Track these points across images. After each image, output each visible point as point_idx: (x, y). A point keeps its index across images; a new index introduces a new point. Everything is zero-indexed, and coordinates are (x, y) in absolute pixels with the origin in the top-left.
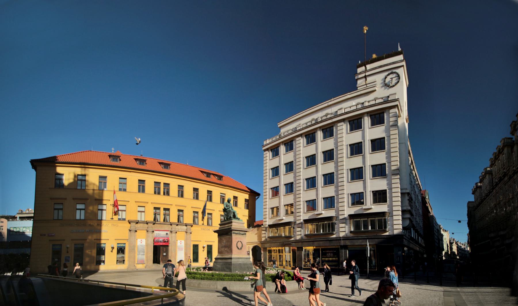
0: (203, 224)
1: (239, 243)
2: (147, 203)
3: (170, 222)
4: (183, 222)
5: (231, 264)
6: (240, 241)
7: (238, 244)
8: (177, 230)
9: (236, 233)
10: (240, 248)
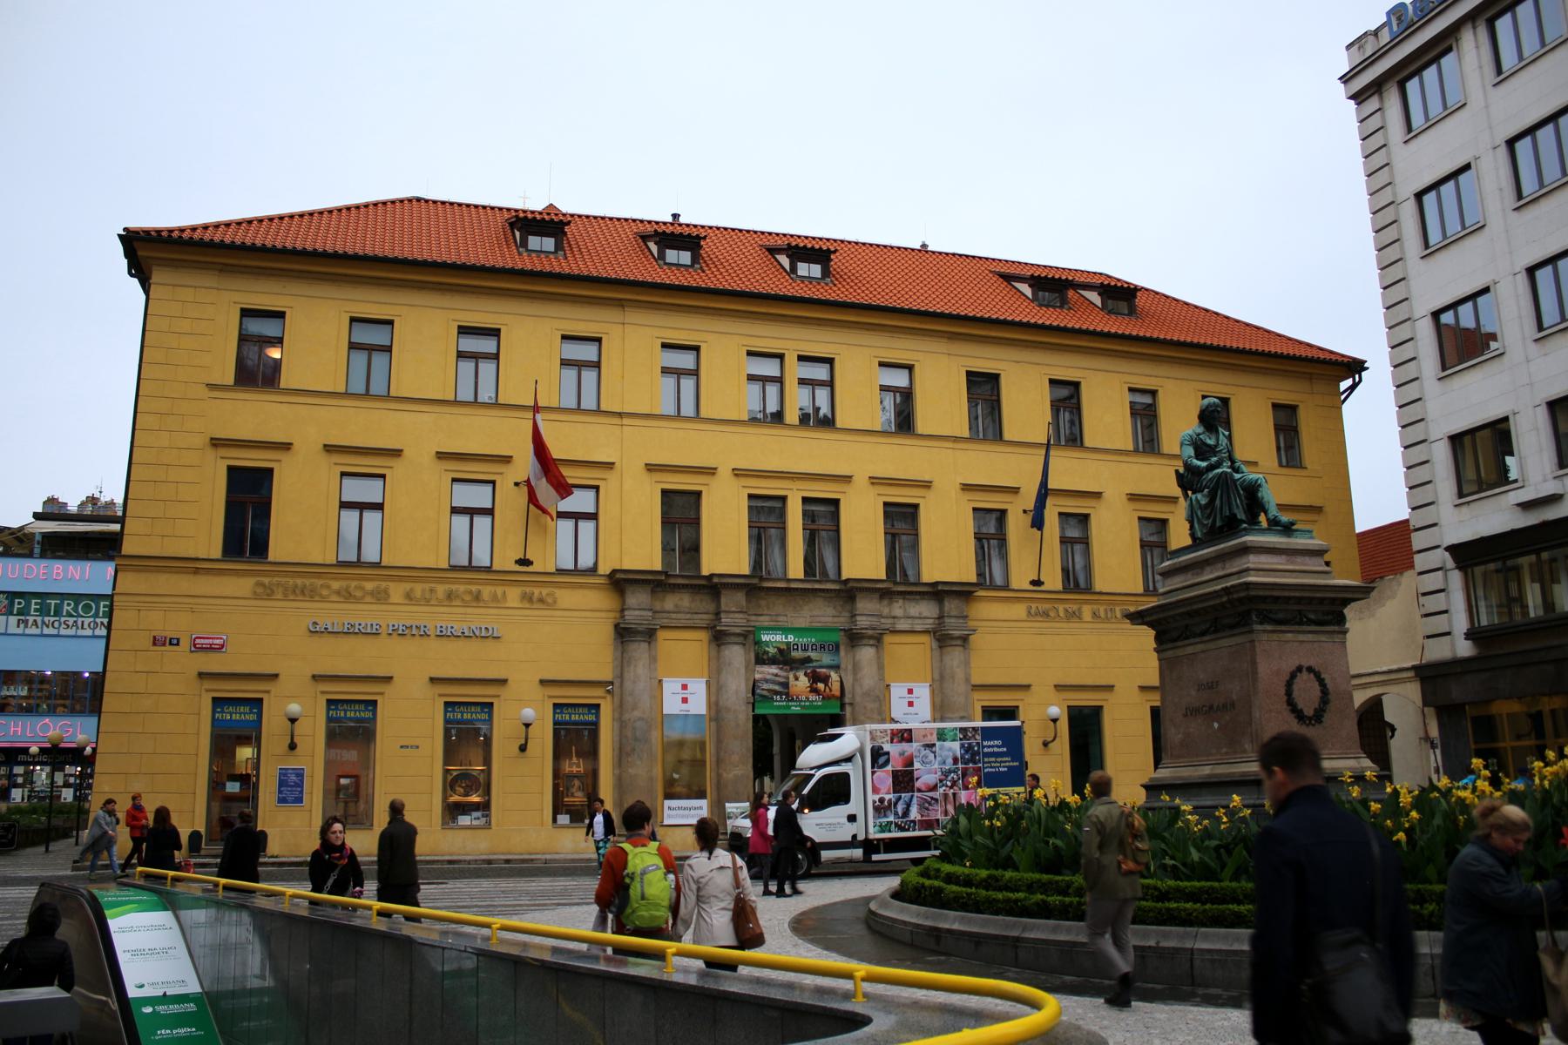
0: (1037, 583)
2: (711, 471)
3: (844, 576)
4: (919, 574)
8: (887, 623)
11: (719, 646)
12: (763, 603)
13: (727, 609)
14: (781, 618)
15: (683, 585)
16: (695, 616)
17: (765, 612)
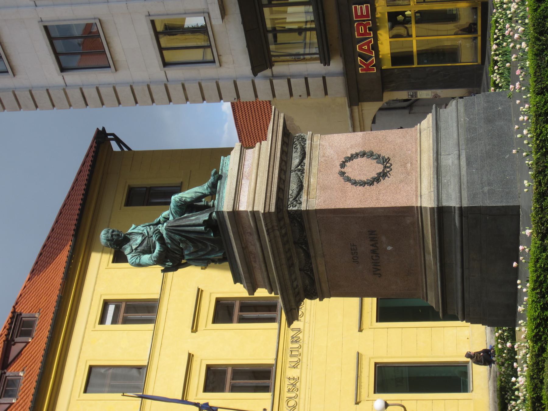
1: (353, 170)
5: (469, 209)
7: (357, 179)
10: (380, 168)
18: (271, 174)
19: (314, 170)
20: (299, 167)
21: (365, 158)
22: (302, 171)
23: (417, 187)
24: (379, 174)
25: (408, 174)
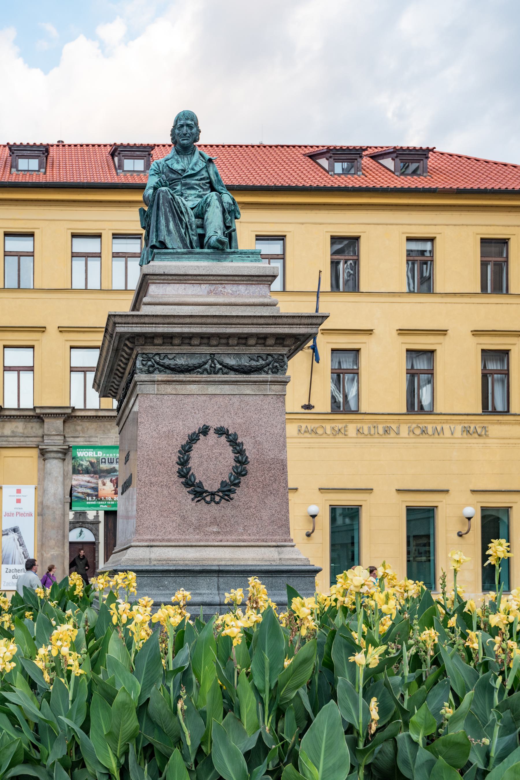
6: (214, 424)
7: (193, 454)
9: (181, 361)
11: (44, 460)
12: (79, 428)
13: (49, 433)
14: (93, 439)
15: (17, 416)
16: (27, 439)
17: (81, 435)
18: (188, 320)
19: (212, 389)
20: (219, 366)
21: (234, 464)
22: (213, 371)
23: (169, 540)
24: (200, 485)
25: (198, 528)
